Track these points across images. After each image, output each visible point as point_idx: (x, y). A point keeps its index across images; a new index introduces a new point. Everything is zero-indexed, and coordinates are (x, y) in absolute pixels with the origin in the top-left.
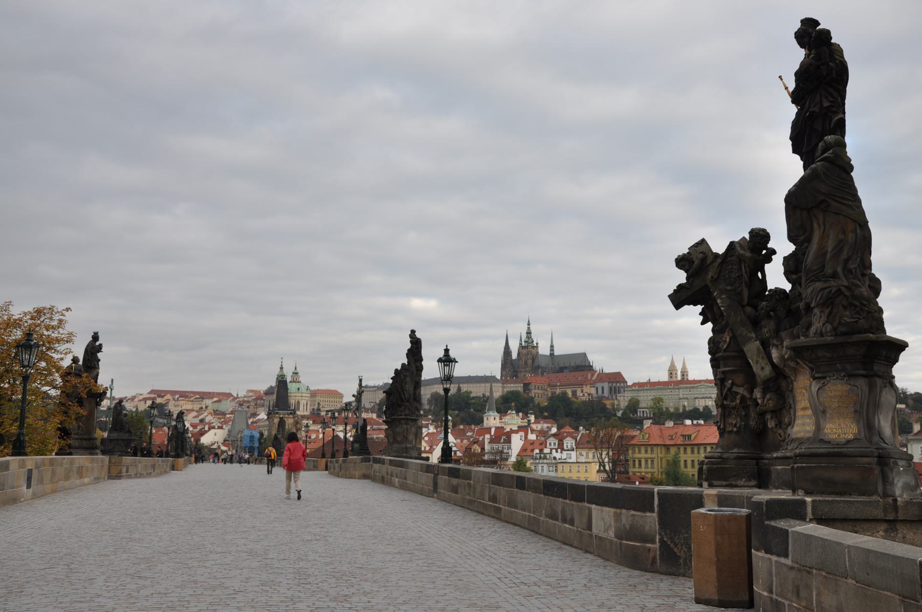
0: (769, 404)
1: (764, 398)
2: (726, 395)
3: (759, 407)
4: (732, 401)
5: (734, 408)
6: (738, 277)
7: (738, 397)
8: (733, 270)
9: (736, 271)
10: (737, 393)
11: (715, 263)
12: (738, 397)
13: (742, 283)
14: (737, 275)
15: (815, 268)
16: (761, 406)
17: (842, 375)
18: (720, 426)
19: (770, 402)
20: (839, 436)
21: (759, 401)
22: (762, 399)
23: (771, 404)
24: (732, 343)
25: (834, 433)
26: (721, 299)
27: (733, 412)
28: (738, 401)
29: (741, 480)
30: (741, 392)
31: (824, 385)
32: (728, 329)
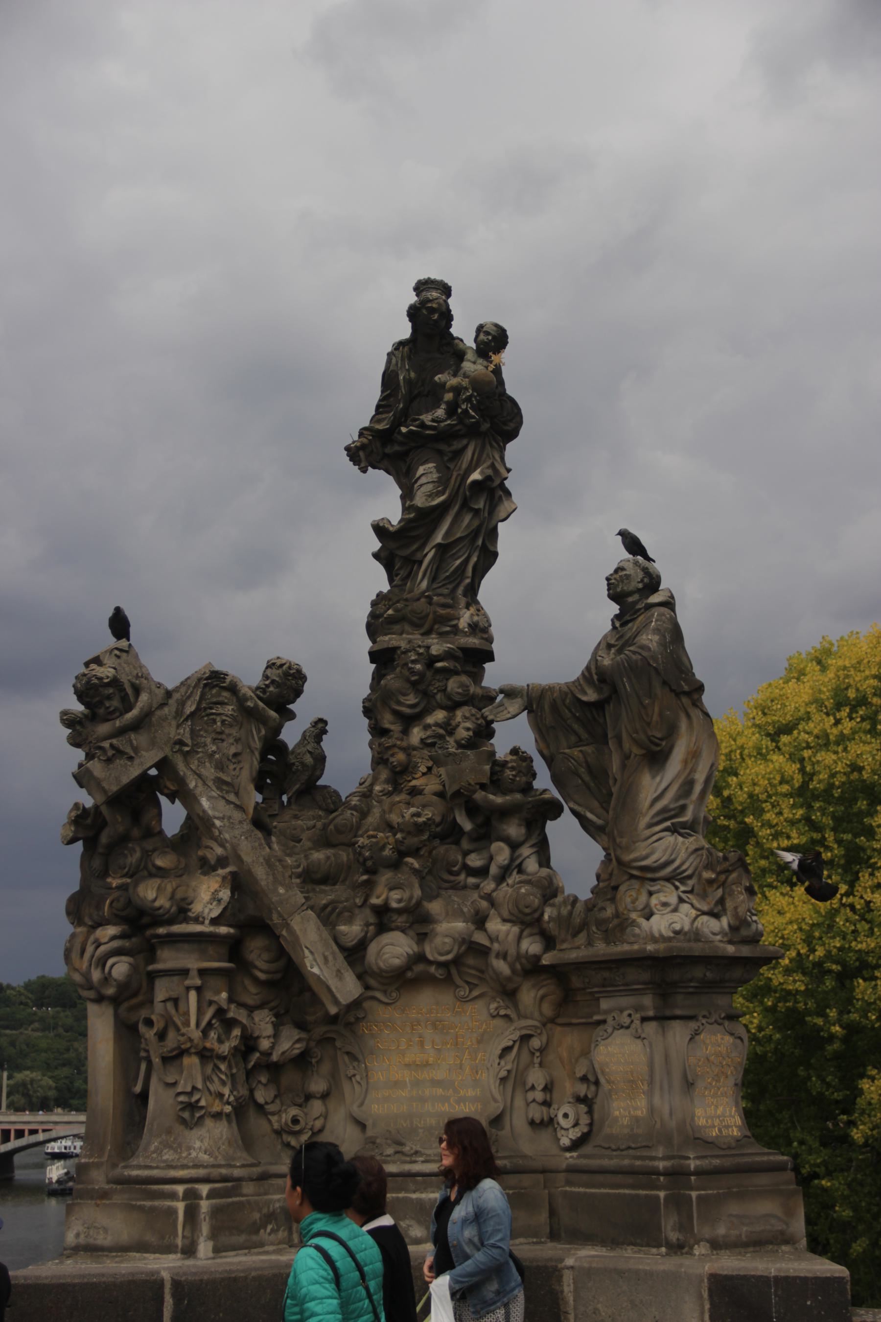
0: (293, 1050)
1: (276, 1036)
2: (210, 1025)
3: (257, 1055)
4: (220, 1041)
5: (223, 1058)
6: (235, 755)
7: (237, 1032)
8: (224, 736)
9: (231, 740)
10: (229, 1024)
11: (166, 710)
12: (237, 1032)
13: (241, 769)
14: (233, 750)
15: (672, 806)
16: (262, 1053)
17: (723, 1015)
18: (198, 1101)
19: (298, 1046)
20: (720, 1130)
21: (265, 1044)
22: (272, 1040)
23: (296, 1052)
24: (230, 906)
25: (710, 1127)
26: (210, 798)
27: (223, 1067)
28: (234, 1043)
29: (265, 1231)
30: (244, 1021)
31: (697, 1033)
32: (221, 872)
